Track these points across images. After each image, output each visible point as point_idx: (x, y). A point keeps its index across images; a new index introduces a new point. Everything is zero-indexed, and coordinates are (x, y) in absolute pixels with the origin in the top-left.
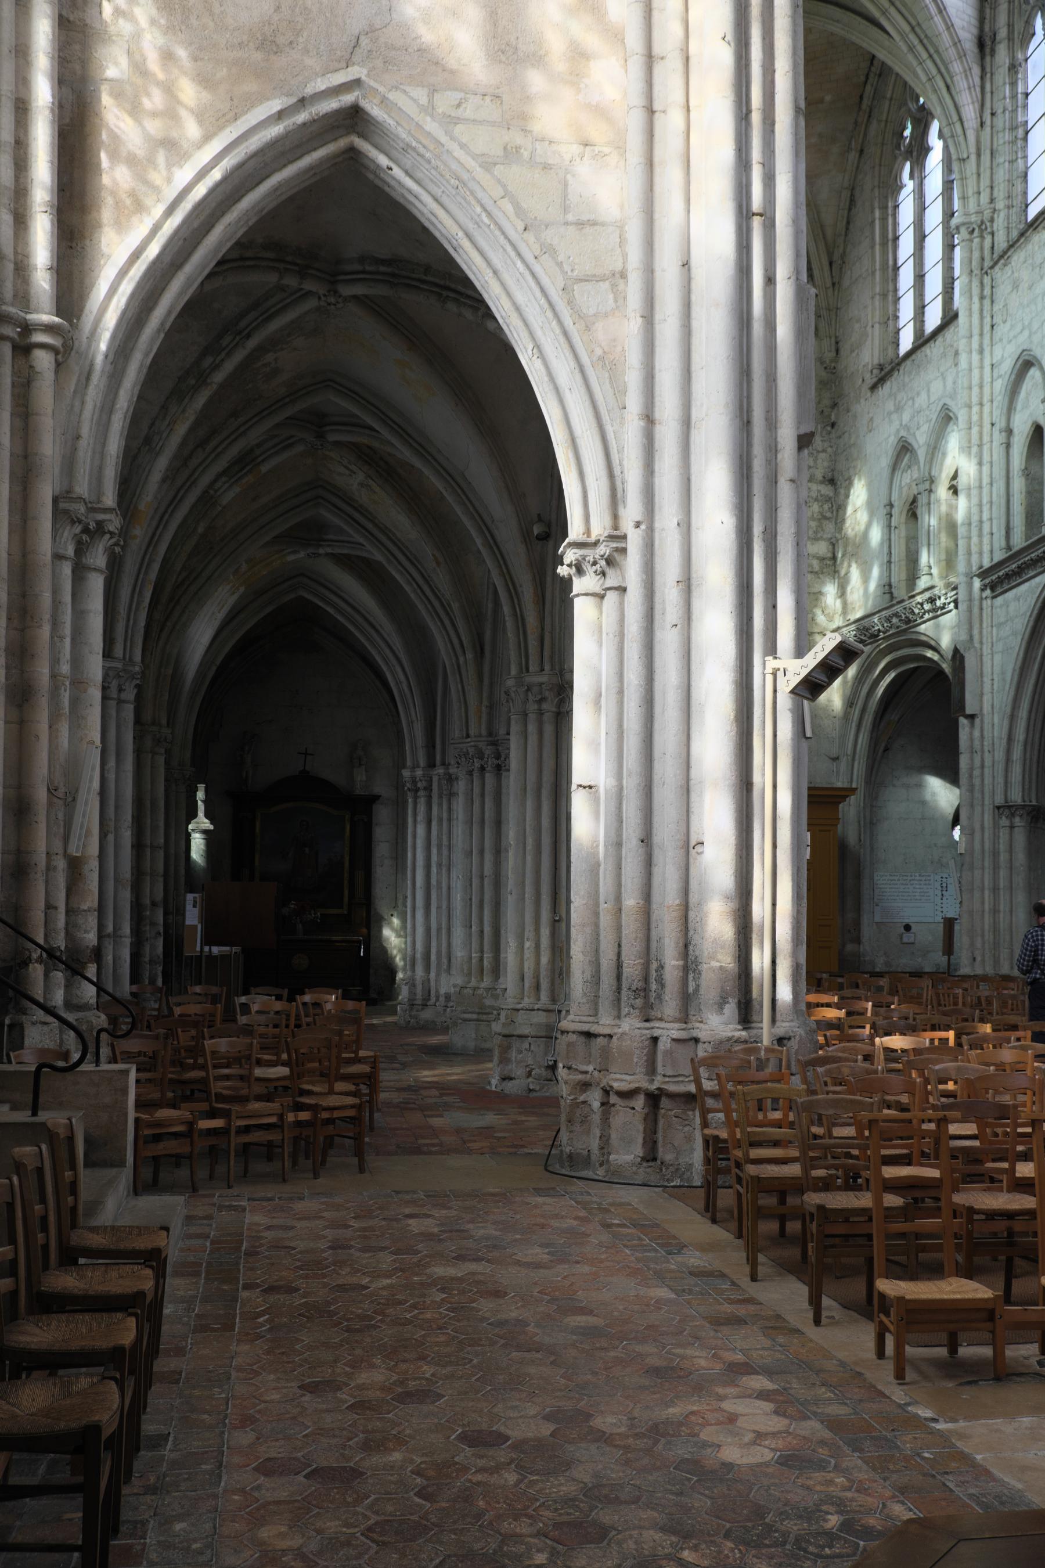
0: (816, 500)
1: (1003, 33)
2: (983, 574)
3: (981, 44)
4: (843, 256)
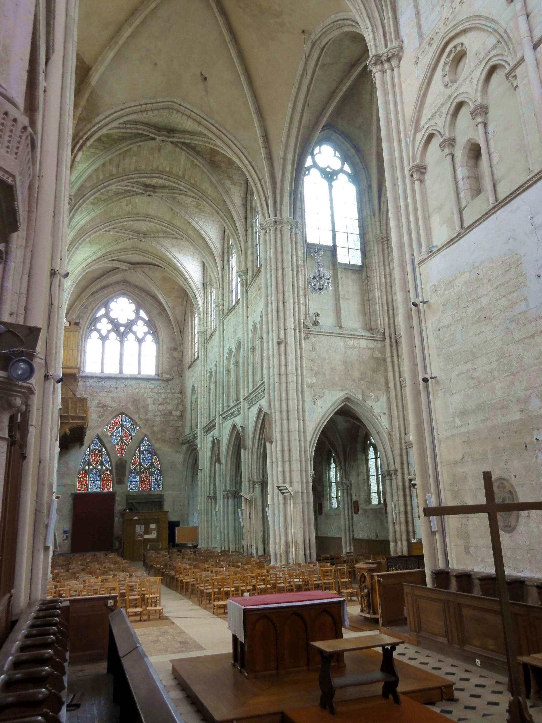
1: (208, 283)
2: (203, 429)
3: (204, 285)
4: (184, 329)
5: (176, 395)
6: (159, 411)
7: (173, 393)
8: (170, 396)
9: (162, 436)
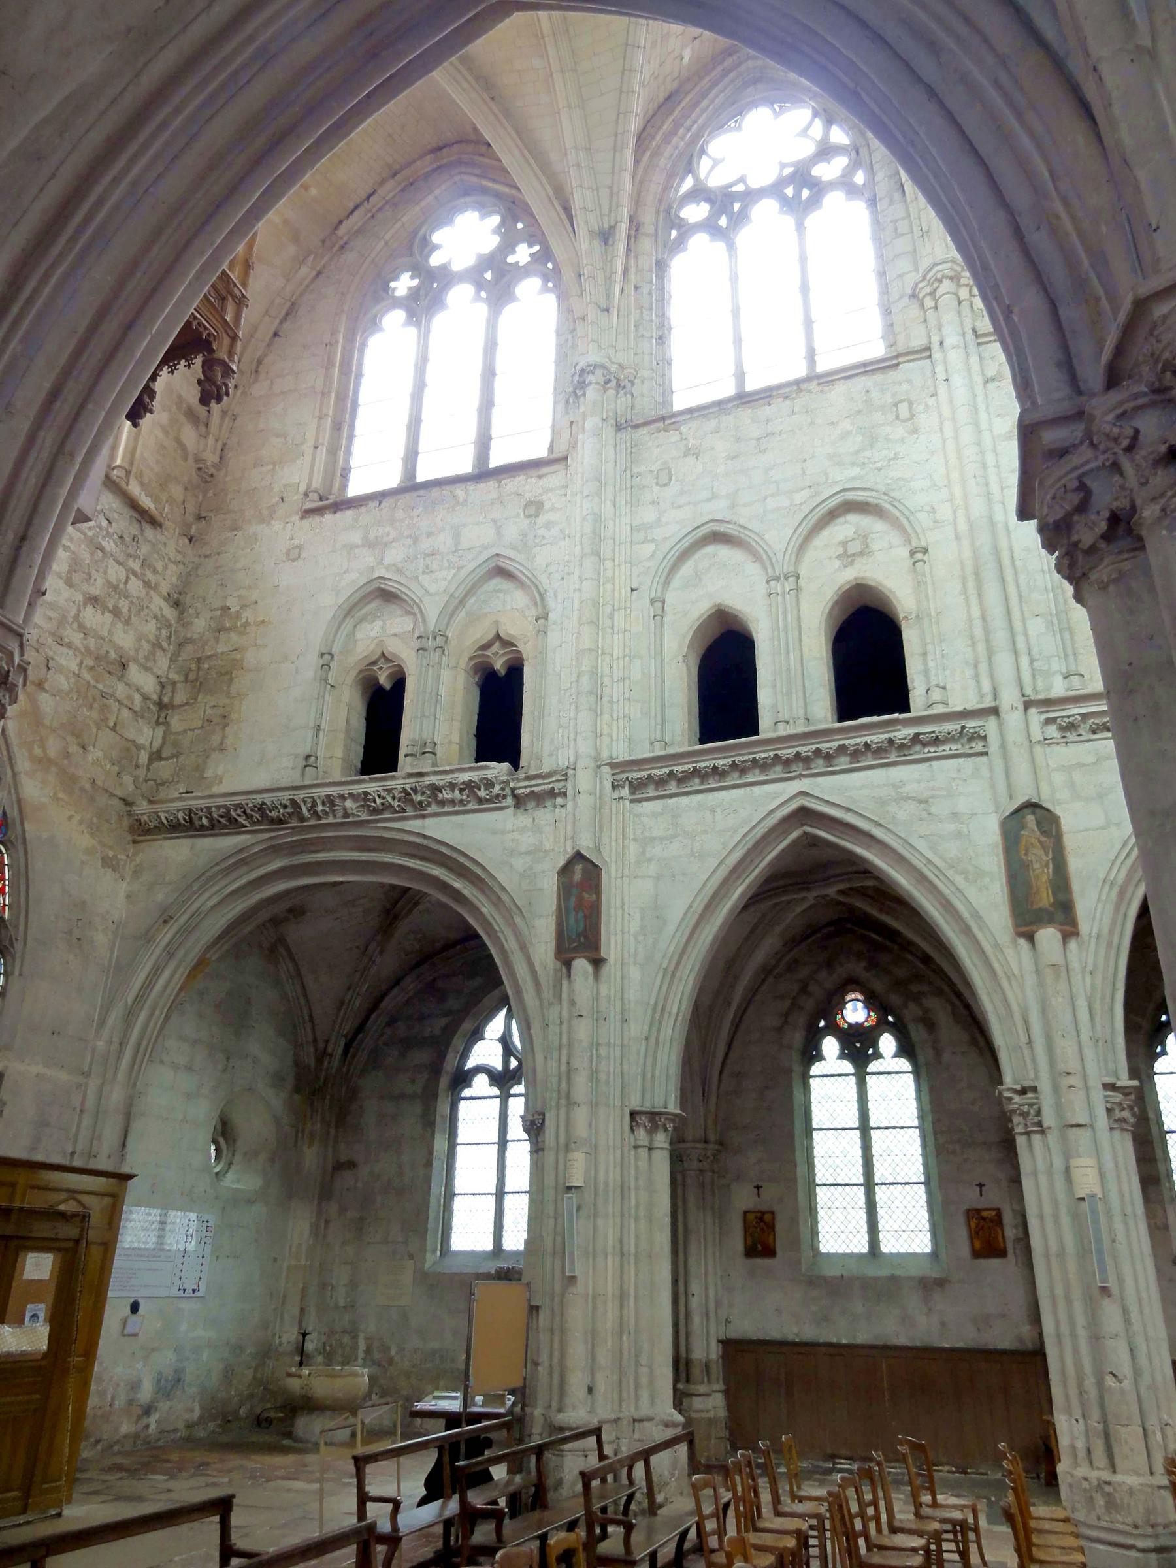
0: (155, 617)
2: (617, 766)
5: (158, 604)
6: (81, 627)
7: (147, 584)
8: (135, 586)
9: (67, 755)
